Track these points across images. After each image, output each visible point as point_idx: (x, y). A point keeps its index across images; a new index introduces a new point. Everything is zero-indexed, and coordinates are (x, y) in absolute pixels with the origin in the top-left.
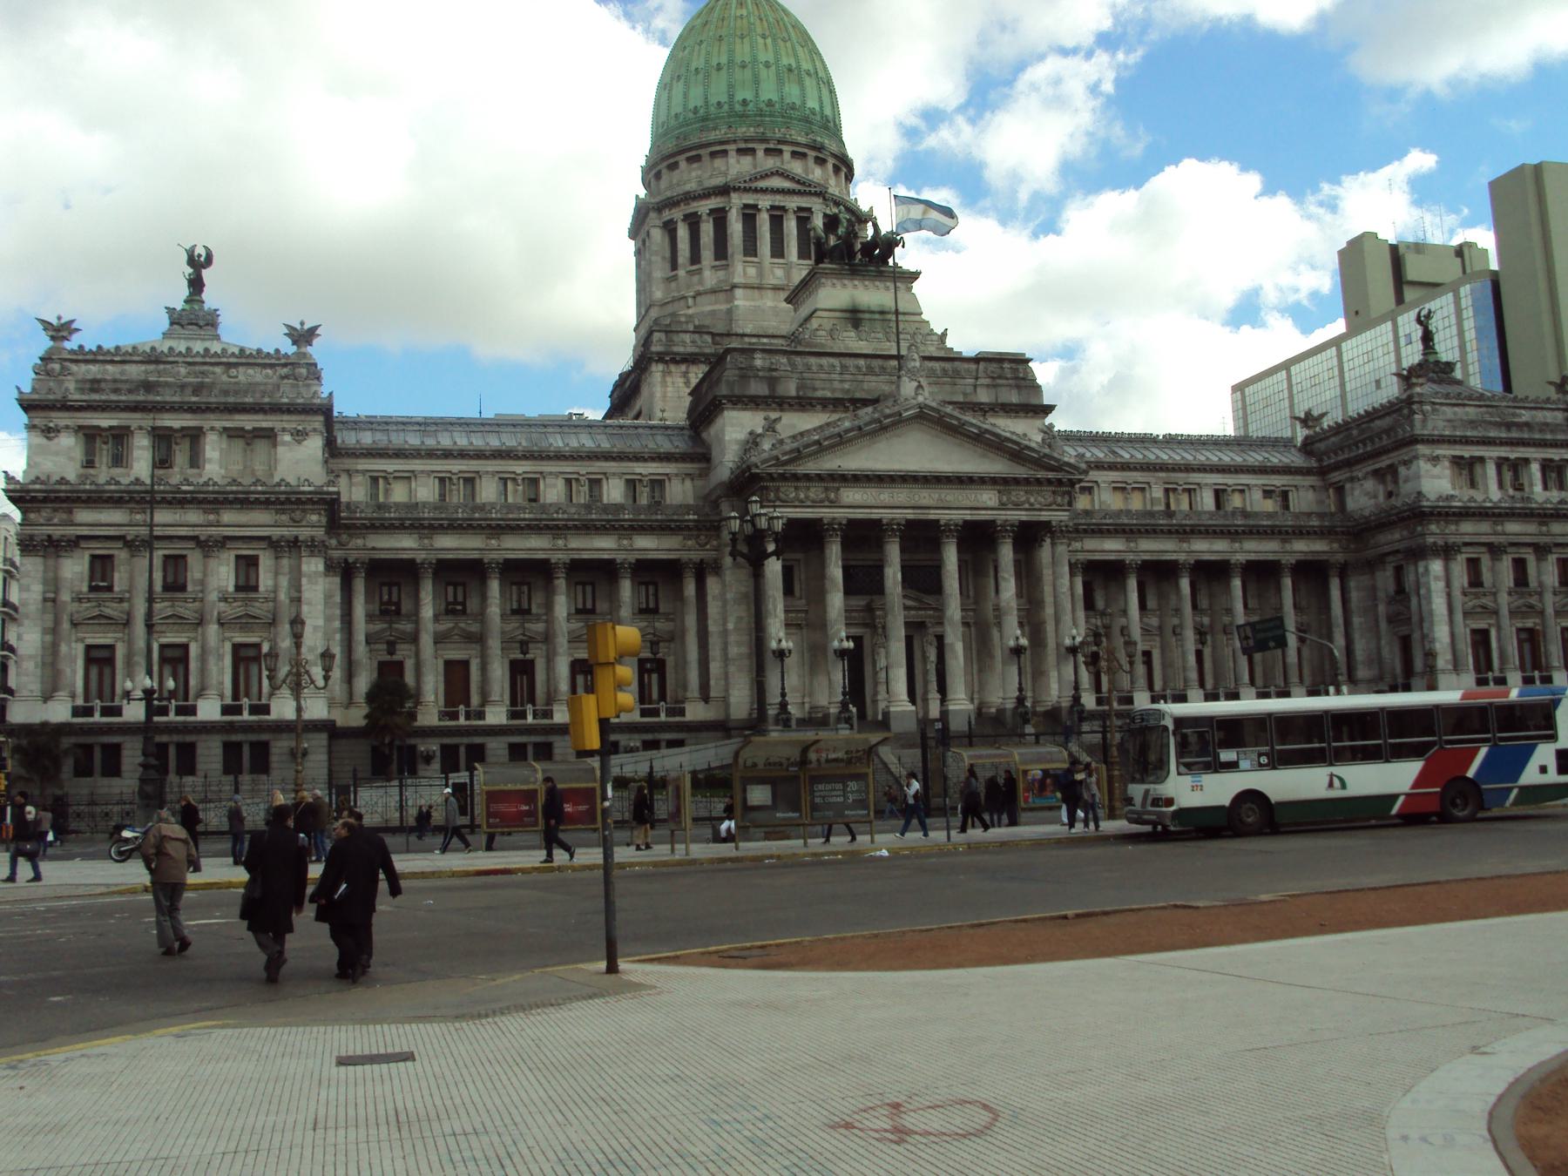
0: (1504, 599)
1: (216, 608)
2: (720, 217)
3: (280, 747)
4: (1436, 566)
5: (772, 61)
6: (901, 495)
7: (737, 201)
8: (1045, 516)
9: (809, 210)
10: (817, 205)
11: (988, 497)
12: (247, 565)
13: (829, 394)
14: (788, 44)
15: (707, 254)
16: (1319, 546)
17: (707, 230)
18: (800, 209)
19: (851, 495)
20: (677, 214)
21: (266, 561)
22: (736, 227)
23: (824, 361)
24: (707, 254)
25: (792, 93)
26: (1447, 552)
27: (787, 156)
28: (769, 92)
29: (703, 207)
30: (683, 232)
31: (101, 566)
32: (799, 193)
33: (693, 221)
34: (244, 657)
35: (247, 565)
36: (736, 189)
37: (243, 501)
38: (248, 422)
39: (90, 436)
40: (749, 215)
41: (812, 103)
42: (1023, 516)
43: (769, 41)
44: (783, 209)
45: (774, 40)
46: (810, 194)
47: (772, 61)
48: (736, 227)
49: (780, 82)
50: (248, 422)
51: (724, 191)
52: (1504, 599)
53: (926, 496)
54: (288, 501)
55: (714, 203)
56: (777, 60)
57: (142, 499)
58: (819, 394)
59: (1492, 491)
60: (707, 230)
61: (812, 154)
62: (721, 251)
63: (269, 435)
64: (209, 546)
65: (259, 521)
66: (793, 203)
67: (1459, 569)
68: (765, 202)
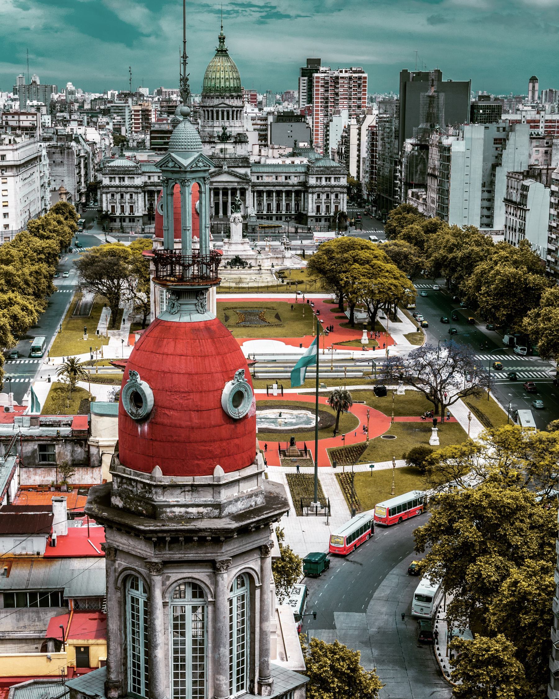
0: (323, 201)
1: (127, 201)
2: (212, 111)
3: (136, 219)
4: (310, 195)
6: (222, 184)
7: (215, 109)
10: (230, 109)
11: (236, 184)
12: (131, 195)
15: (210, 118)
16: (300, 188)
17: (210, 113)
19: (214, 184)
20: (205, 109)
21: (134, 194)
22: (215, 115)
24: (210, 118)
25: (227, 84)
26: (313, 193)
28: (222, 85)
29: (210, 109)
30: (206, 113)
31: (113, 195)
33: (208, 111)
34: (131, 207)
35: (131, 195)
37: (131, 187)
38: (131, 176)
39: (110, 178)
40: (217, 112)
41: (232, 85)
48: (215, 115)
49: (225, 82)
50: (131, 176)
51: (212, 107)
52: (323, 201)
53: (226, 184)
54: (137, 187)
55: (211, 109)
57: (117, 187)
59: (324, 183)
60: (210, 113)
62: (213, 119)
63: (133, 178)
64: (127, 193)
65: (133, 190)
66: (225, 109)
67: (315, 196)
68: (220, 109)
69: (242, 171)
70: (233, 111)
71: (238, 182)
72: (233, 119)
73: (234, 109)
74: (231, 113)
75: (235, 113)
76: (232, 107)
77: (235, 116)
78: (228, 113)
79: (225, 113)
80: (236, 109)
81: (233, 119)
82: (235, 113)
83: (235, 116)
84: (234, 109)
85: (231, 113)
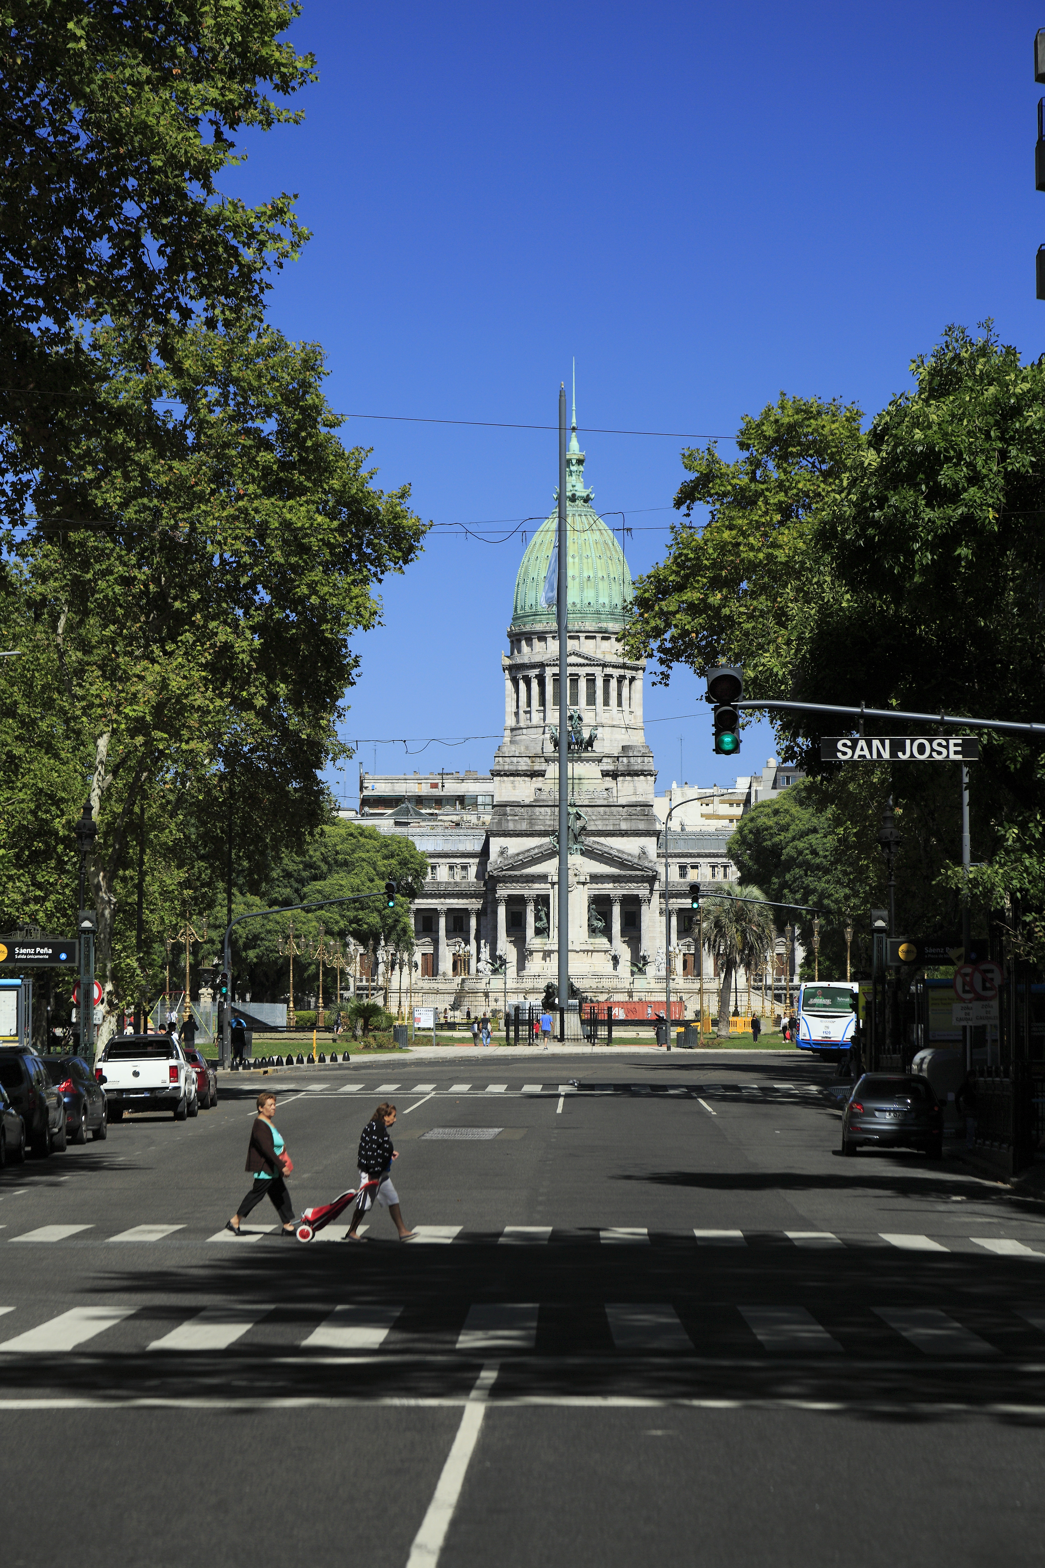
5: (577, 575)
8: (635, 892)
9: (593, 675)
10: (598, 671)
13: (543, 828)
14: (590, 560)
18: (588, 675)
23: (542, 809)
27: (582, 639)
29: (533, 673)
32: (588, 665)
36: (548, 665)
41: (604, 599)
42: (625, 892)
43: (577, 560)
44: (577, 675)
45: (581, 559)
46: (594, 665)
47: (577, 575)
49: (582, 590)
55: (536, 671)
56: (581, 573)
58: (537, 828)
60: (535, 684)
61: (599, 635)
69: (629, 846)
70: (607, 679)
71: (614, 879)
72: (606, 703)
73: (609, 671)
74: (599, 683)
75: (613, 683)
76: (604, 666)
77: (613, 694)
78: (591, 680)
79: (582, 684)
80: (616, 673)
81: (606, 703)
82: (613, 683)
83: (613, 694)
84: (609, 671)
85: (599, 683)
